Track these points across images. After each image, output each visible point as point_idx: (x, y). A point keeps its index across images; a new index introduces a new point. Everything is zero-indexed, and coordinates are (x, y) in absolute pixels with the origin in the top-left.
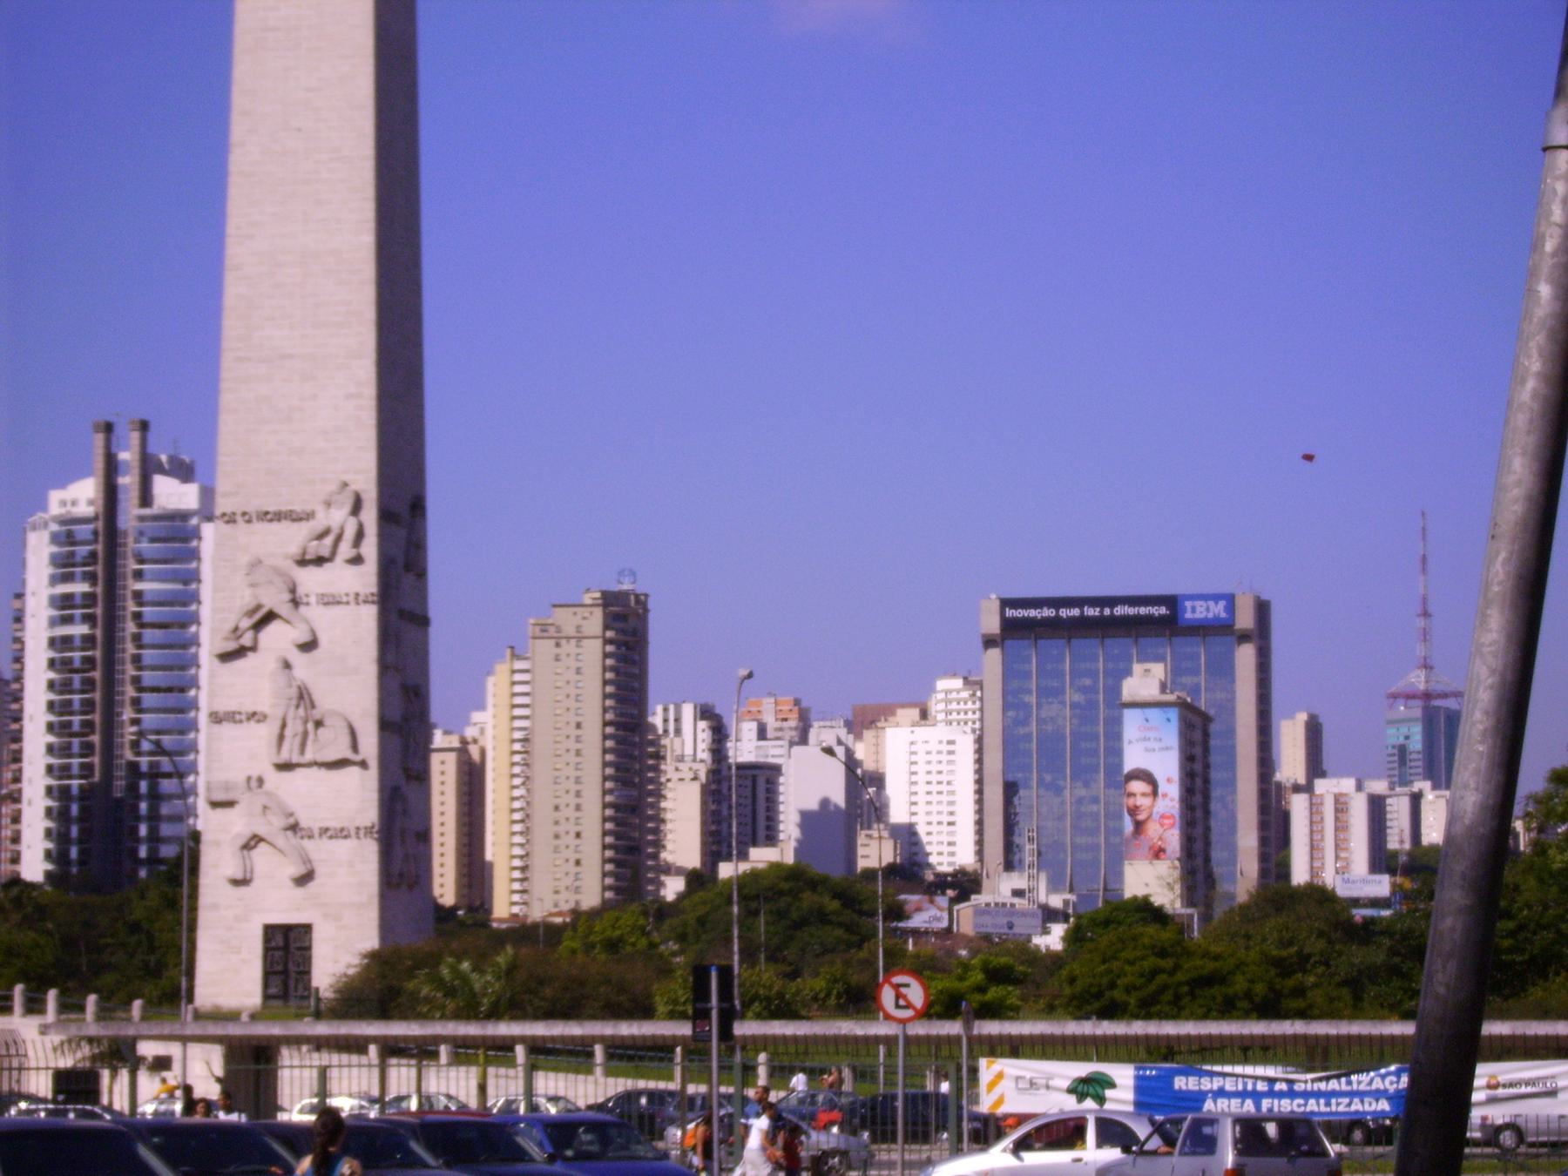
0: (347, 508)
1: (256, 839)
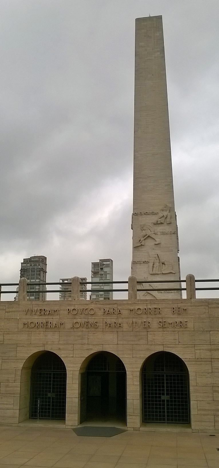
0: (168, 211)
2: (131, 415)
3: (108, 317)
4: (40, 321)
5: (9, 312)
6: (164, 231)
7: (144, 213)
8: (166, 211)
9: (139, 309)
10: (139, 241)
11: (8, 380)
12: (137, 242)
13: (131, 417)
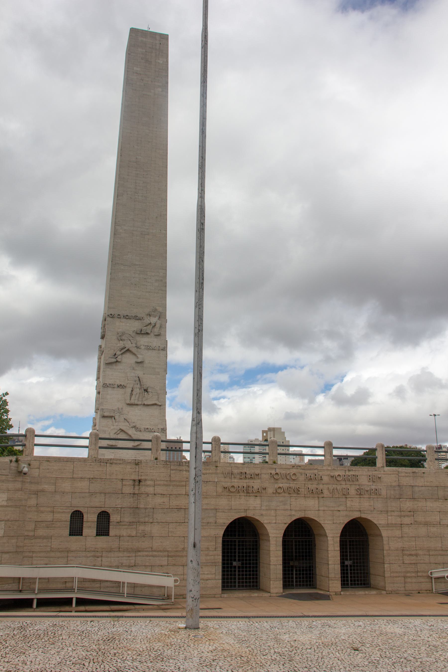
0: (157, 318)
1: (120, 431)
2: (333, 580)
3: (309, 483)
4: (241, 485)
5: (206, 474)
6: (150, 344)
7: (124, 316)
8: (155, 317)
9: (339, 475)
10: (114, 356)
11: (208, 548)
12: (112, 356)
13: (333, 582)
